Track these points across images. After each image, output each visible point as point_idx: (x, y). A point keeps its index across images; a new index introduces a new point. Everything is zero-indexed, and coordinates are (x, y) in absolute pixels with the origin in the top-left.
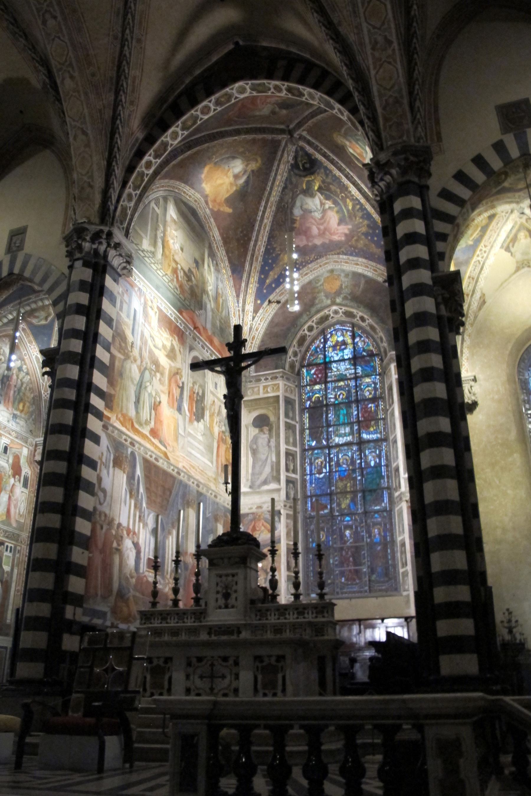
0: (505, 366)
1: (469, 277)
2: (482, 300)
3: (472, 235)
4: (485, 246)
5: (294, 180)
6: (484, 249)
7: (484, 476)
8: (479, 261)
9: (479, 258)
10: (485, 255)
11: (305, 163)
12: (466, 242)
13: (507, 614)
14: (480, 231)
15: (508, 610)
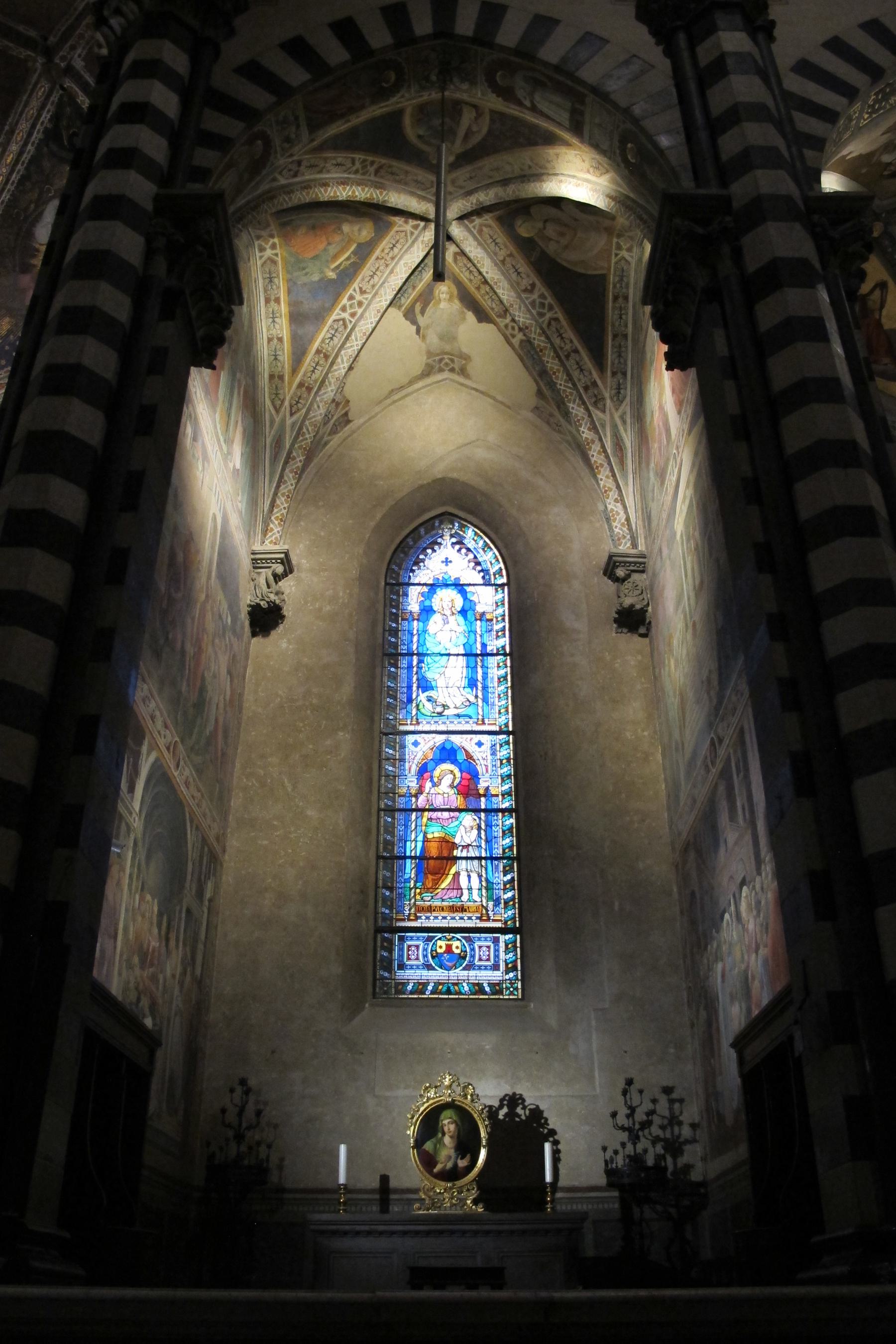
0: (360, 550)
1: (318, 352)
2: (340, 412)
3: (335, 257)
4: (362, 292)
5: (46, 164)
6: (358, 297)
7: (262, 772)
8: (344, 320)
9: (345, 315)
10: (360, 311)
11: (75, 134)
12: (322, 272)
13: (239, 1090)
14: (354, 253)
15: (243, 1082)
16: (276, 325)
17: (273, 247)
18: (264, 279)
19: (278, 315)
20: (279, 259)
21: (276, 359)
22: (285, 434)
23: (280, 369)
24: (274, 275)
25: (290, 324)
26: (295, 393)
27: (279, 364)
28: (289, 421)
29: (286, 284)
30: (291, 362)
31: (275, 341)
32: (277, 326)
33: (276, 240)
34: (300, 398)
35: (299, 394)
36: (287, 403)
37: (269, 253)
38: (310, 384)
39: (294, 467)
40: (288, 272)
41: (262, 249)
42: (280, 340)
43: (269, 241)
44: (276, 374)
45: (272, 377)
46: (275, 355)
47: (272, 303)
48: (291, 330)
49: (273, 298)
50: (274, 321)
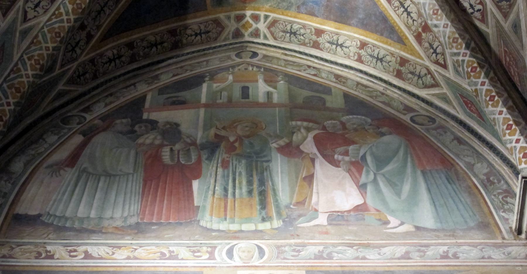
16: (346, 44)
17: (256, 18)
18: (290, 42)
19: (335, 38)
20: (272, 15)
21: (381, 60)
22: (460, 86)
23: (394, 59)
24: (289, 28)
25: (350, 25)
26: (426, 50)
27: (388, 58)
28: (451, 74)
29: (301, 15)
30: (390, 41)
31: (362, 52)
32: (348, 44)
33: (248, 13)
34: (431, 46)
35: (427, 45)
36: (433, 67)
37: (262, 26)
38: (421, 24)
39: (484, 97)
40: (288, 8)
41: (257, 33)
42: (363, 45)
43: (248, 22)
44: (398, 67)
45: (399, 75)
46: (378, 59)
47: (321, 40)
48: (357, 26)
49: (314, 37)
50: (341, 46)
